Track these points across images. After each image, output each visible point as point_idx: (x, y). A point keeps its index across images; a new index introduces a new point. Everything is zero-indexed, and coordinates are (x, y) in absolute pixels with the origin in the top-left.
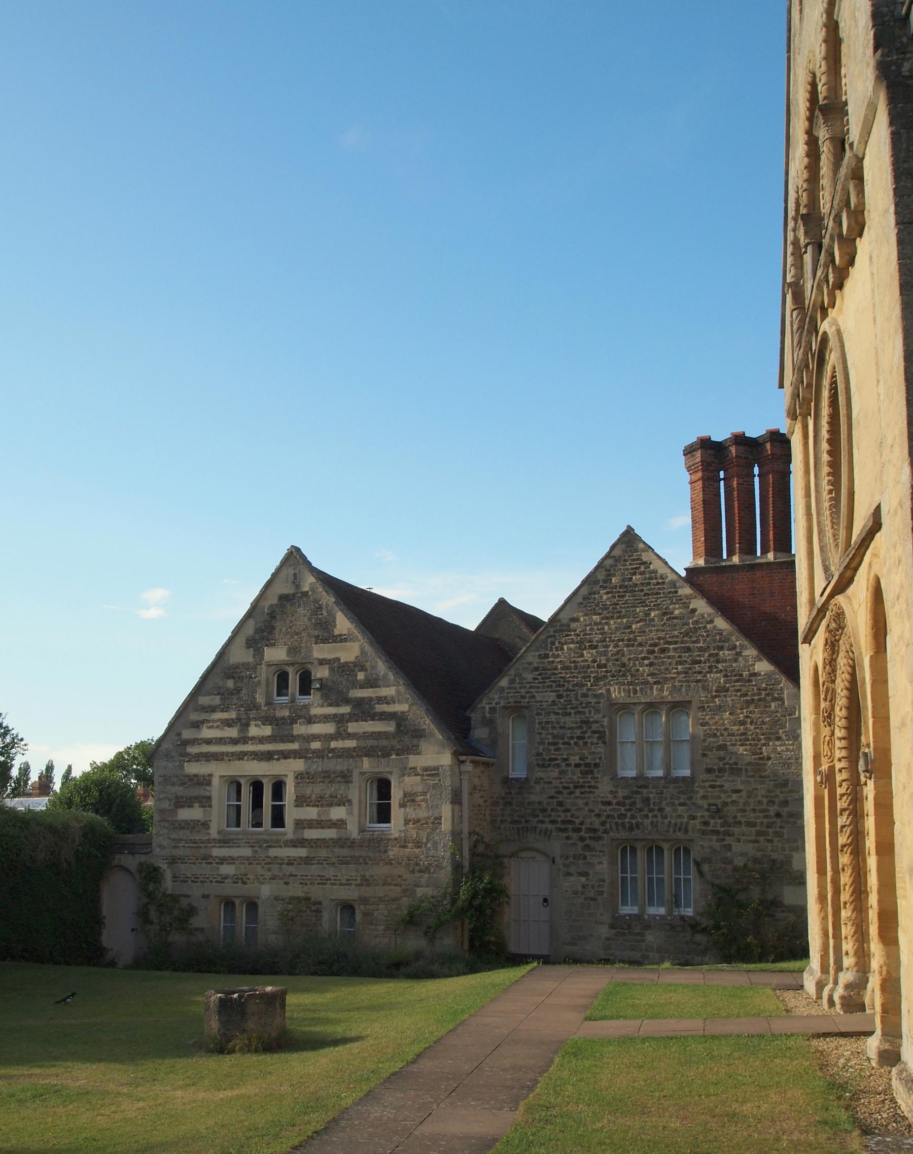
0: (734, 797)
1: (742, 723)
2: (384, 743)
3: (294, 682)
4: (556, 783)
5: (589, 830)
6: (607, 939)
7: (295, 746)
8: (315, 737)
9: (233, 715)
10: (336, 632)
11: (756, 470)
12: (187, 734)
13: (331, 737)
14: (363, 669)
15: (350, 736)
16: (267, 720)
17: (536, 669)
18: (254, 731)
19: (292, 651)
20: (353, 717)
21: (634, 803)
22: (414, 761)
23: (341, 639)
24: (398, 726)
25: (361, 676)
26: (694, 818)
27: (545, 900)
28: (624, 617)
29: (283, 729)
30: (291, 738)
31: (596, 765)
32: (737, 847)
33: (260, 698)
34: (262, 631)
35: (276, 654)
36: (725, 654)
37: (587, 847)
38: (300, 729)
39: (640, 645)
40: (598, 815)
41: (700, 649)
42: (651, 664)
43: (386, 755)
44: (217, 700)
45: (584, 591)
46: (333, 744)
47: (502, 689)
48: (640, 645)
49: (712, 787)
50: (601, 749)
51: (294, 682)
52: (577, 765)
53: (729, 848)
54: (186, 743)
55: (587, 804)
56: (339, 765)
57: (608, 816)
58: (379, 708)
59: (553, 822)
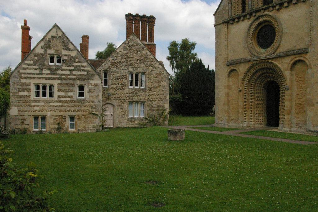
0: (154, 93)
1: (156, 78)
2: (84, 77)
3: (55, 60)
4: (115, 89)
5: (123, 99)
6: (127, 123)
7: (58, 76)
8: (64, 75)
9: (38, 67)
10: (69, 48)
11: (141, 23)
12: (22, 71)
13: (68, 75)
14: (77, 58)
15: (73, 75)
16: (48, 69)
17: (111, 62)
18: (45, 71)
19: (56, 51)
20: (73, 70)
21: (133, 94)
22: (91, 82)
23: (69, 50)
24: (87, 73)
25: (77, 60)
26: (146, 97)
27: (112, 115)
28: (132, 52)
29: (53, 71)
30: (56, 74)
31: (125, 85)
32: (154, 103)
33: (46, 63)
34: (46, 45)
35: (51, 52)
36: (153, 63)
37: (123, 103)
38: (59, 72)
39: (135, 59)
40: (125, 96)
41: (148, 61)
42: (138, 64)
43: (84, 80)
44: (32, 62)
45: (123, 45)
46: (69, 77)
47: (103, 66)
48: (135, 59)
49: (150, 91)
50: (126, 81)
51: (55, 60)
52: (120, 85)
53: (152, 103)
54: (22, 74)
55: (123, 93)
56: (72, 82)
57: (127, 96)
58: (82, 68)
59: (115, 97)
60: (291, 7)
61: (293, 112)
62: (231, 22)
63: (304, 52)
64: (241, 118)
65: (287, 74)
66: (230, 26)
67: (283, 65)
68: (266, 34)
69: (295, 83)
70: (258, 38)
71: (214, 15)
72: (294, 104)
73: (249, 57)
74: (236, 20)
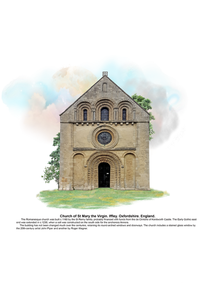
60: (125, 125)
61: (125, 179)
62: (77, 124)
63: (134, 149)
64: (86, 184)
65: (122, 159)
66: (75, 126)
67: (120, 154)
68: (104, 137)
69: (126, 164)
70: (98, 138)
71: (60, 115)
72: (126, 175)
73: (93, 148)
74: (82, 124)
